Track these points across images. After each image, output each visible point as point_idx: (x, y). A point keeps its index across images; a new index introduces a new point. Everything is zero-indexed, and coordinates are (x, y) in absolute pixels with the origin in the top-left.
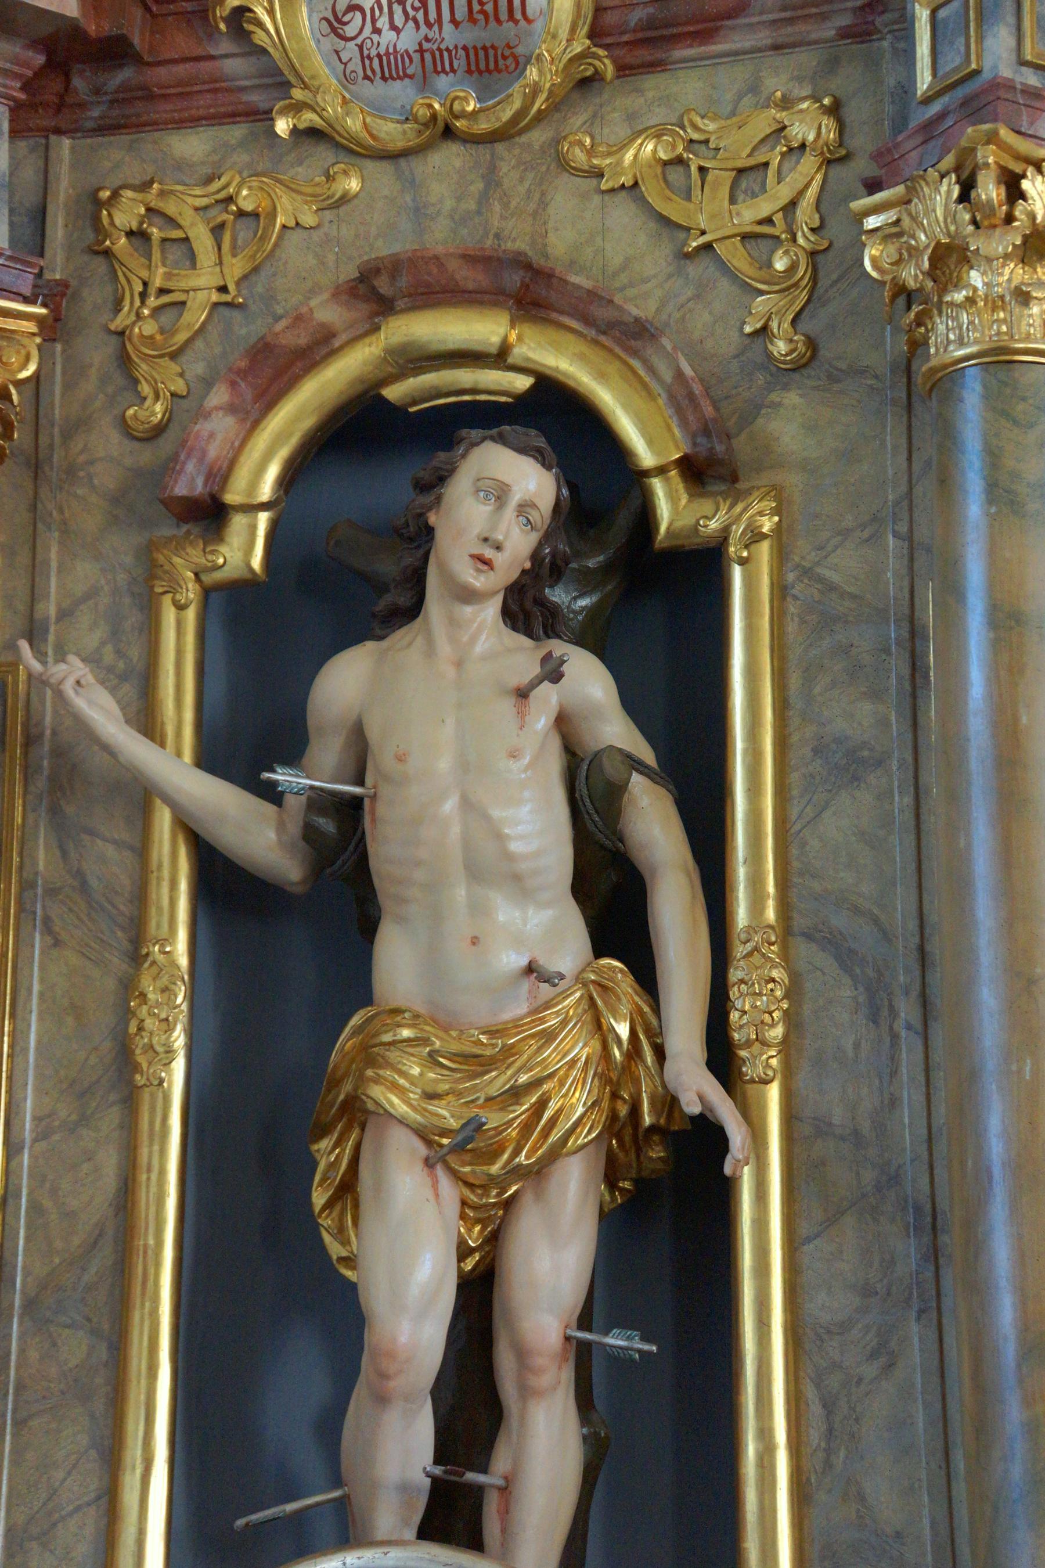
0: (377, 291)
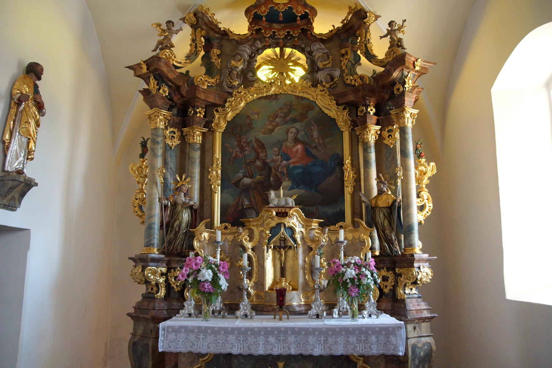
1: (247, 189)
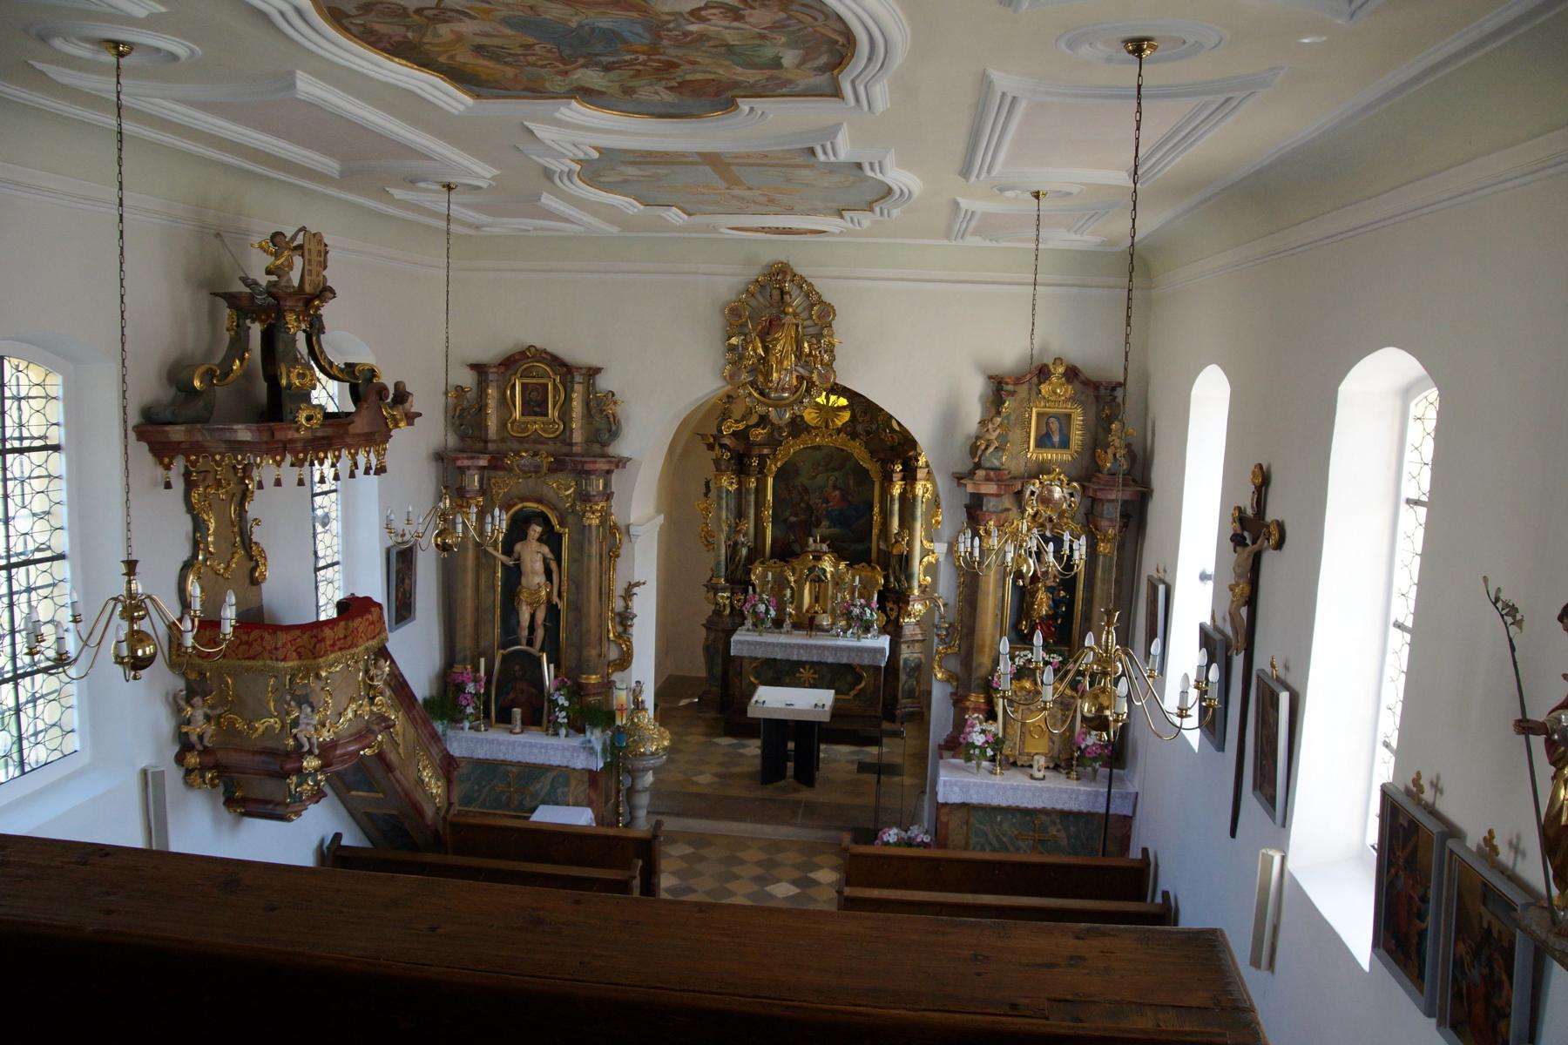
0: (523, 499)
1: (792, 526)
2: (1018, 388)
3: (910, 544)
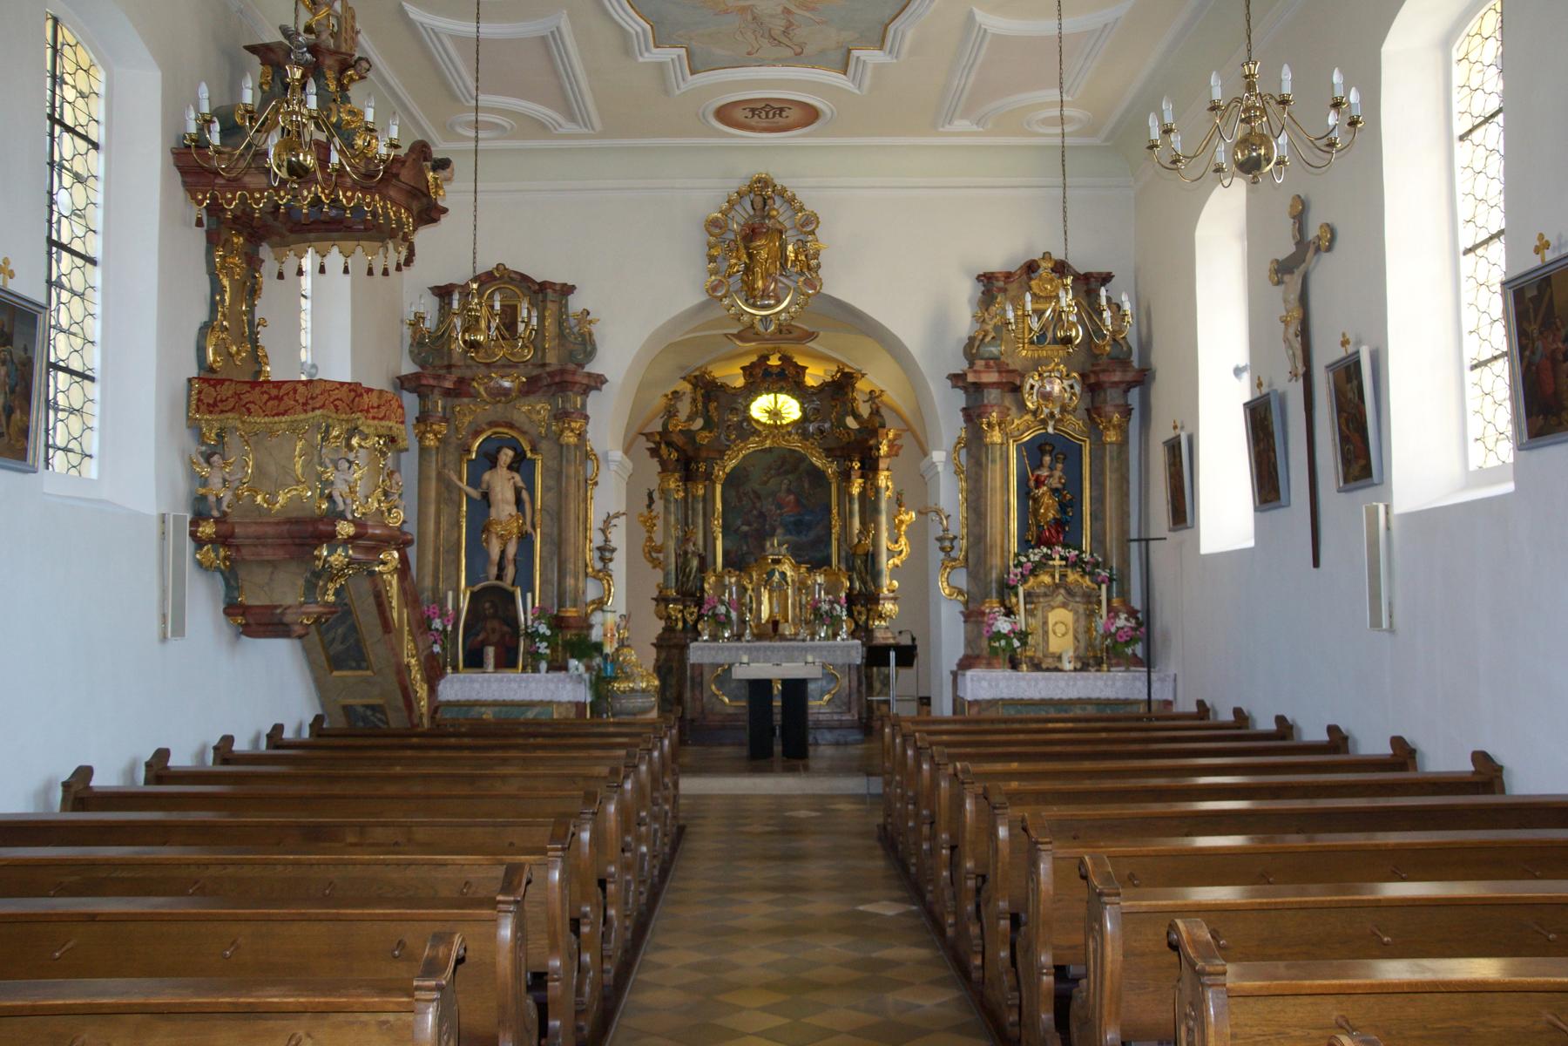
1: (745, 535)
2: (1009, 287)
3: (876, 542)
